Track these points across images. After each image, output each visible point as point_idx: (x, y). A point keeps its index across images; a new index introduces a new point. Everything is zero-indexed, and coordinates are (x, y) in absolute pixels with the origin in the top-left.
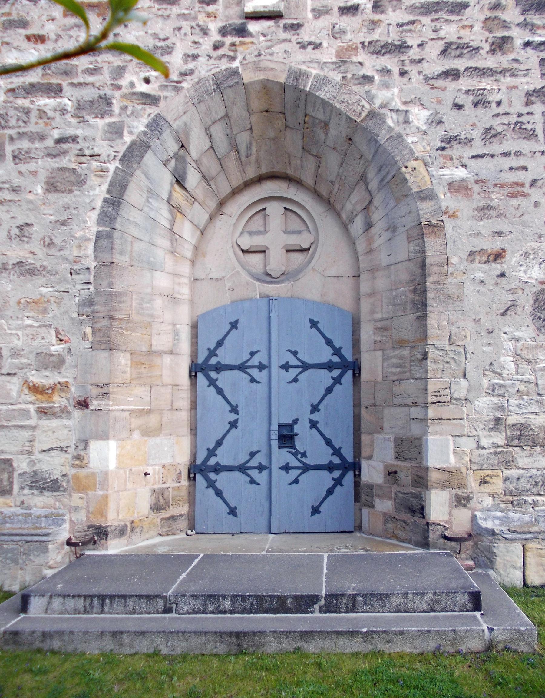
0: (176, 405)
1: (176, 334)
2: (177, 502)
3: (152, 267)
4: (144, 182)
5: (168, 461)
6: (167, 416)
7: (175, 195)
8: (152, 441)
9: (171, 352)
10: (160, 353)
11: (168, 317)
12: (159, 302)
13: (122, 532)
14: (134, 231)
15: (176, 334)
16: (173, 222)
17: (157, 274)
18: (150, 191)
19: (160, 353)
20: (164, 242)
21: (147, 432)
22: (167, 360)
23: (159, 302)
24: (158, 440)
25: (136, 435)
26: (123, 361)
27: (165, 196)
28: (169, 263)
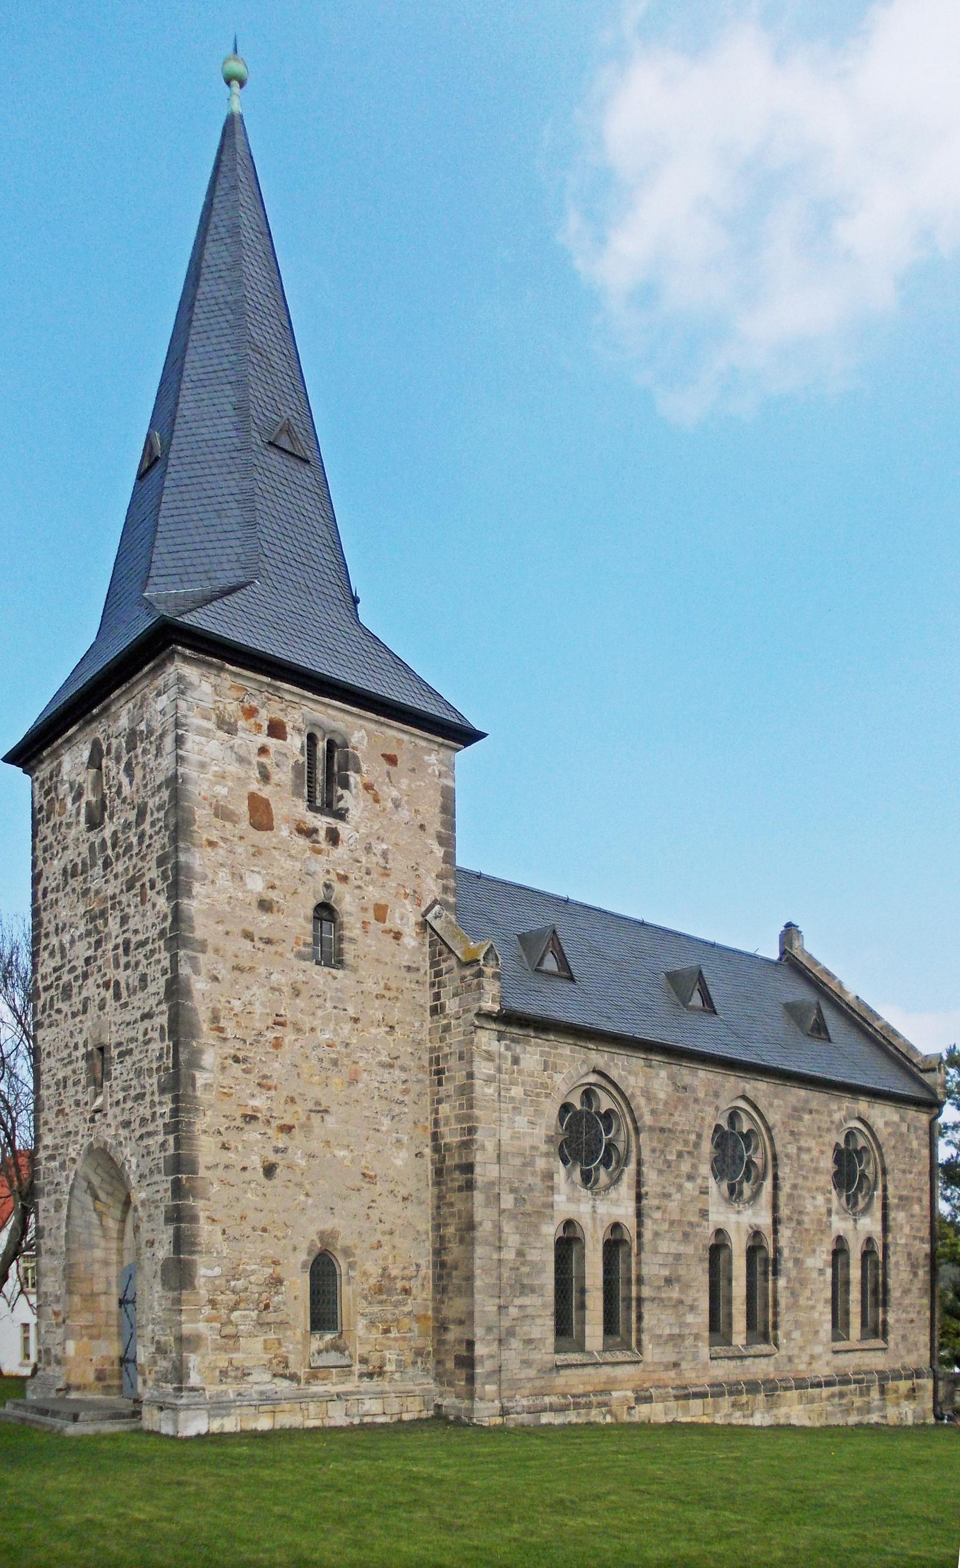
0: (111, 1322)
1: (109, 1283)
2: (112, 1377)
3: (92, 1246)
4: (78, 1204)
5: (105, 1353)
6: (104, 1329)
7: (97, 1206)
8: (94, 1343)
9: (105, 1293)
10: (99, 1294)
11: (103, 1273)
12: (97, 1266)
13: (78, 1388)
14: (79, 1230)
15: (109, 1283)
16: (101, 1221)
17: (95, 1250)
18: (82, 1208)
19: (99, 1294)
20: (99, 1232)
21: (91, 1337)
22: (103, 1298)
23: (97, 1266)
24: (99, 1342)
25: (85, 1339)
26: (76, 1300)
27: (92, 1208)
28: (103, 1243)
